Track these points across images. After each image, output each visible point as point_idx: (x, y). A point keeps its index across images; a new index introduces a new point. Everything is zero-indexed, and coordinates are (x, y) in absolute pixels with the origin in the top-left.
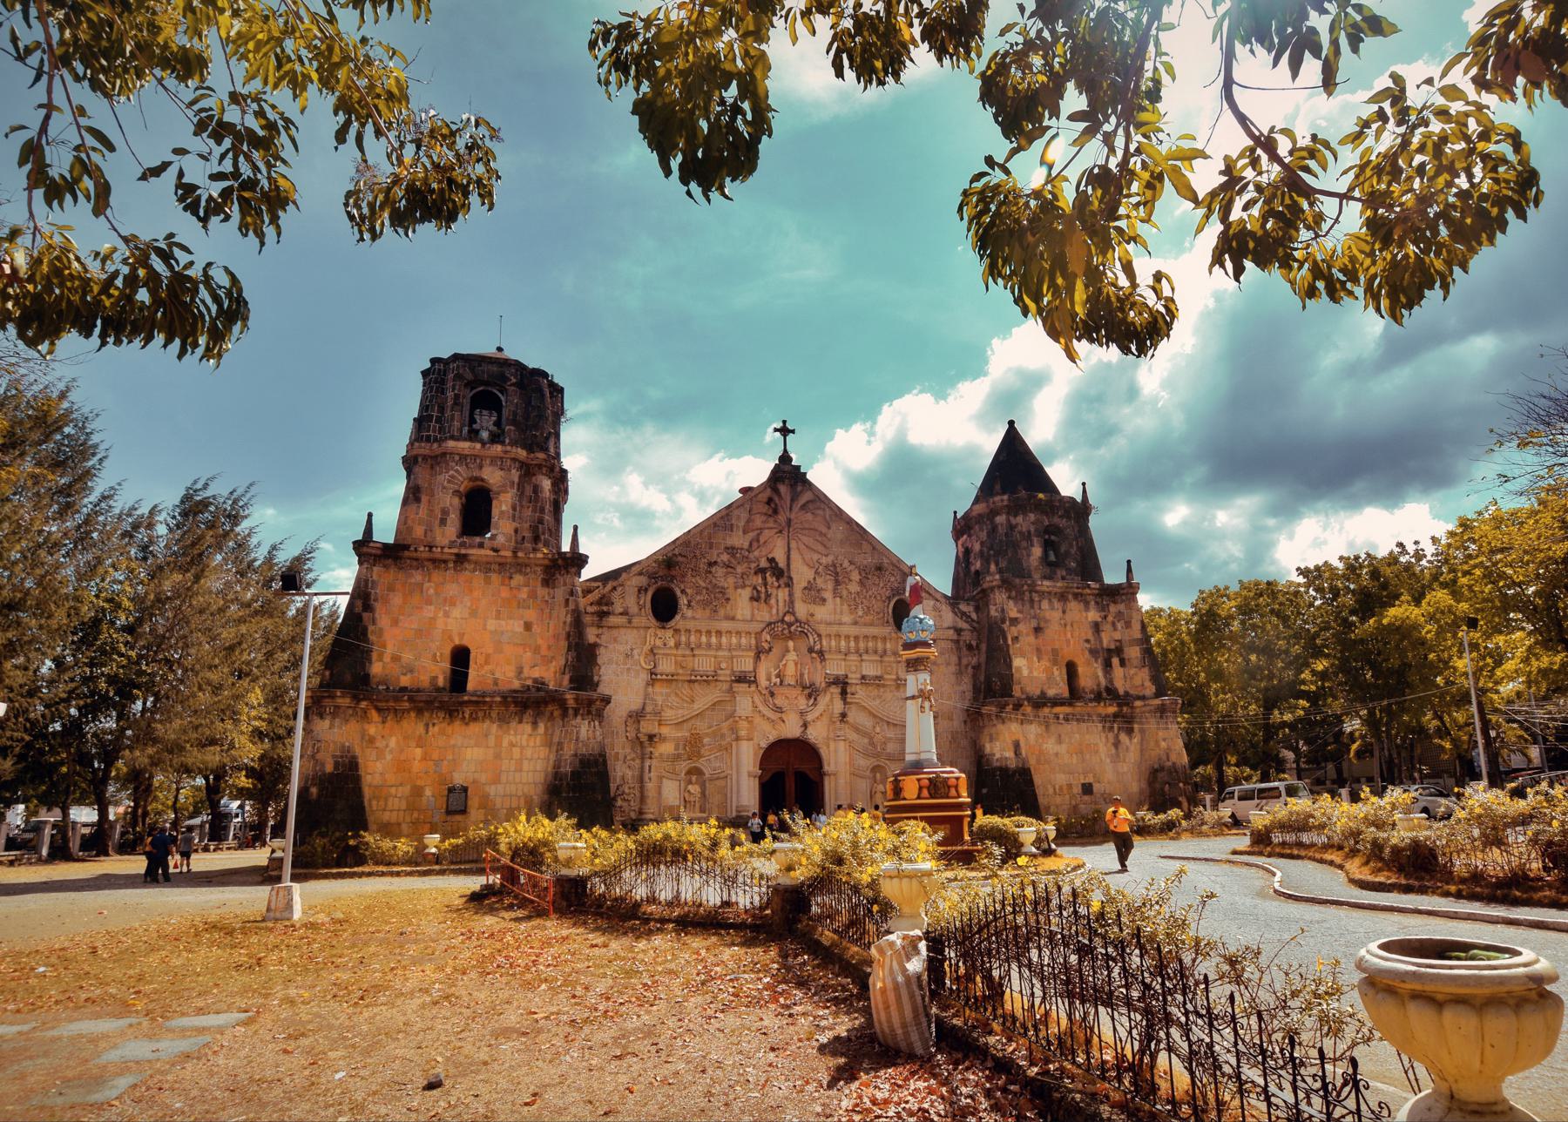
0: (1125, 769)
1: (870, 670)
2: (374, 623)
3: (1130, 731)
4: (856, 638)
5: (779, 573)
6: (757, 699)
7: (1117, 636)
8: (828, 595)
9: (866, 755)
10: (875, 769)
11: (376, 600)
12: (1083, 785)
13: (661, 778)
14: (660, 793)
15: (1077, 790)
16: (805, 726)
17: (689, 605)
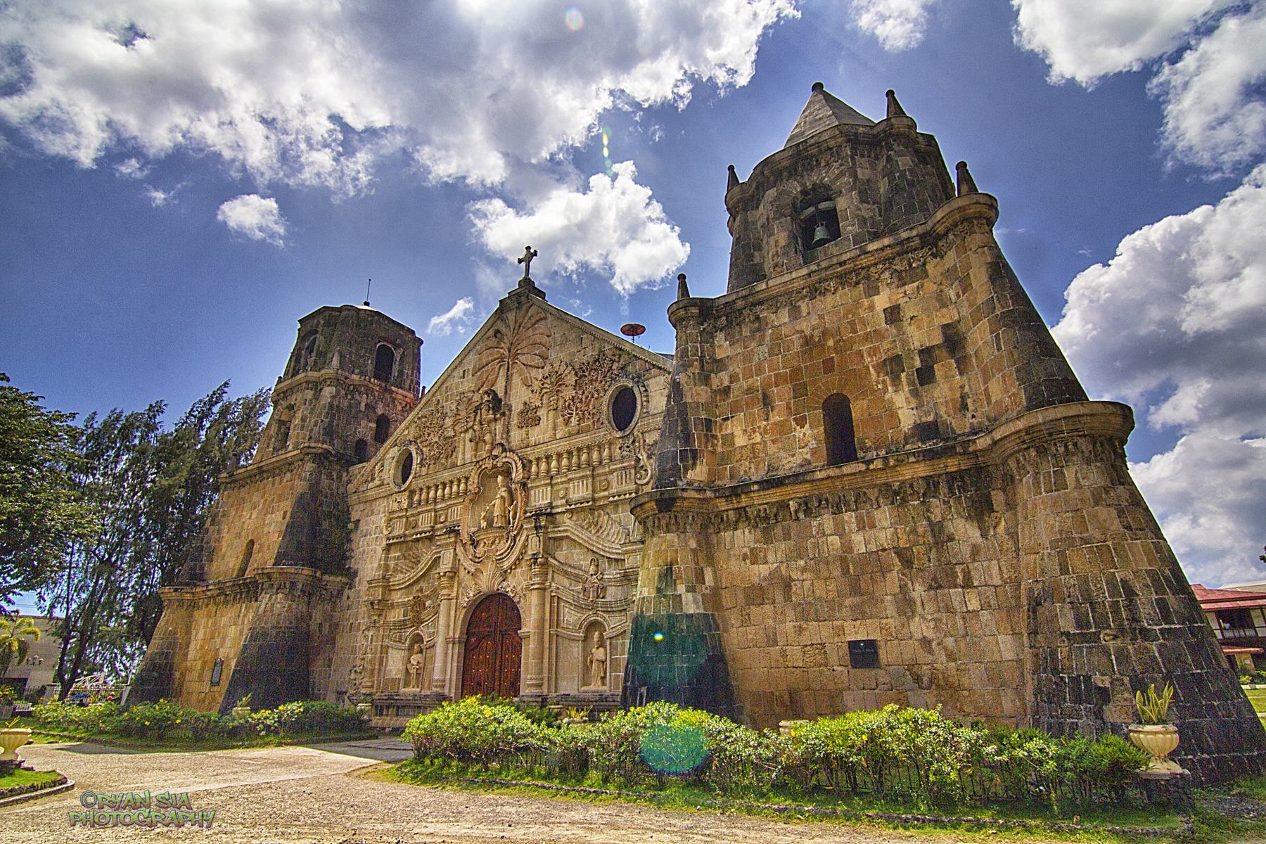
0: (974, 604)
1: (579, 492)
2: (219, 532)
3: (981, 510)
4: (570, 453)
5: (497, 404)
6: (459, 549)
7: (948, 316)
8: (541, 413)
9: (579, 608)
10: (594, 625)
11: (223, 516)
12: (853, 645)
13: (385, 649)
14: (381, 664)
15: (837, 655)
16: (505, 575)
17: (421, 464)
